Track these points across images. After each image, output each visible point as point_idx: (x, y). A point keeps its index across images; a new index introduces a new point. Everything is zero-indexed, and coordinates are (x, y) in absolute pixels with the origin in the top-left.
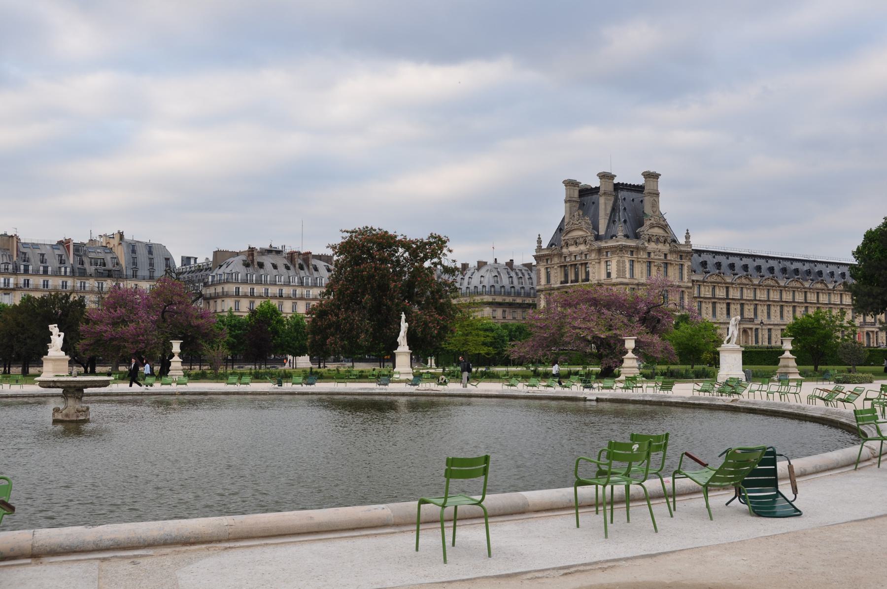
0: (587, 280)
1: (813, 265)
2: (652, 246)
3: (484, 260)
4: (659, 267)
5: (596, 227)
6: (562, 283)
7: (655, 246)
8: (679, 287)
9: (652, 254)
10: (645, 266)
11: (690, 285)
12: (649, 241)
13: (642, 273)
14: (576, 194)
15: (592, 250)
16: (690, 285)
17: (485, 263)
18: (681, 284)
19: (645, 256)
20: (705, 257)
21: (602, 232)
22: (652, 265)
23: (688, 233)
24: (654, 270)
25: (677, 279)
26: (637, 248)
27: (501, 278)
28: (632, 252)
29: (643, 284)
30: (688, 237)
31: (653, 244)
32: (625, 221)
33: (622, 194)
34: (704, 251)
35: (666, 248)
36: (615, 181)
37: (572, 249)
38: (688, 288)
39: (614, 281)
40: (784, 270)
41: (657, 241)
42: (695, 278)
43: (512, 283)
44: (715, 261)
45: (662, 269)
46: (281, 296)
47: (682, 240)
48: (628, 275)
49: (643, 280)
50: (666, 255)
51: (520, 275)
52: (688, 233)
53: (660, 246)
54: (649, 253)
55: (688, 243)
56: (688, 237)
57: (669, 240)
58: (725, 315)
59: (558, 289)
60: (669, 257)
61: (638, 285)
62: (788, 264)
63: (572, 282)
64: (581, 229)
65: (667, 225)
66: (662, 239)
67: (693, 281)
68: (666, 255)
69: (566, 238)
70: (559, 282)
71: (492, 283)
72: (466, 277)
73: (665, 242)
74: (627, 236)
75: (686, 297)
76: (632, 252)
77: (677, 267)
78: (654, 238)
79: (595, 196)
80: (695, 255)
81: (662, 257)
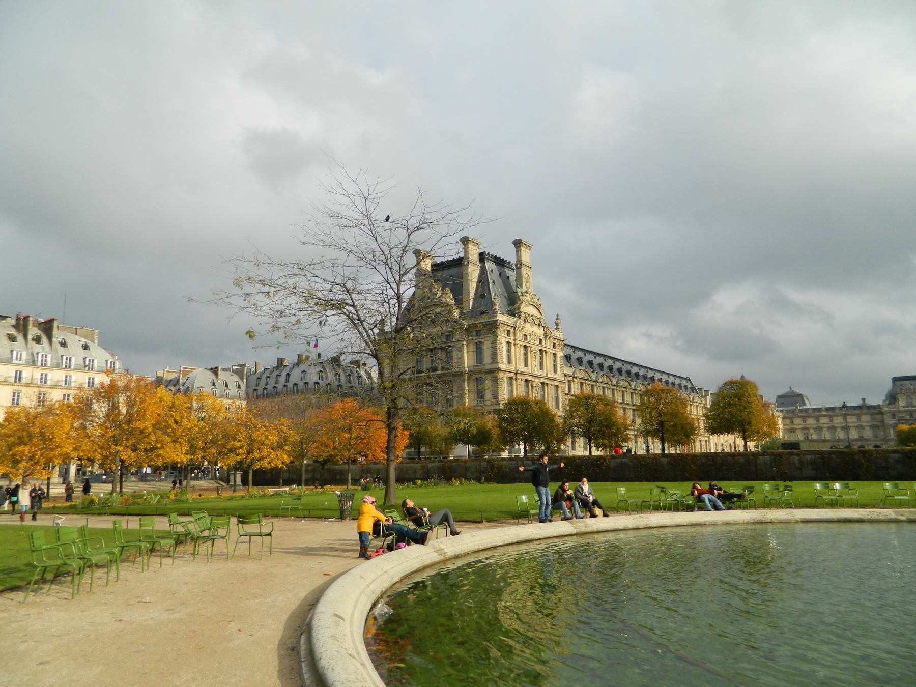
2: (528, 328)
9: (528, 338)
14: (429, 268)
19: (522, 338)
27: (326, 374)
29: (522, 373)
35: (540, 332)
39: (487, 367)
40: (629, 373)
43: (339, 380)
50: (540, 340)
51: (348, 372)
53: (535, 328)
62: (629, 367)
67: (565, 375)
71: (316, 379)
74: (503, 313)
75: (560, 393)
78: (530, 319)
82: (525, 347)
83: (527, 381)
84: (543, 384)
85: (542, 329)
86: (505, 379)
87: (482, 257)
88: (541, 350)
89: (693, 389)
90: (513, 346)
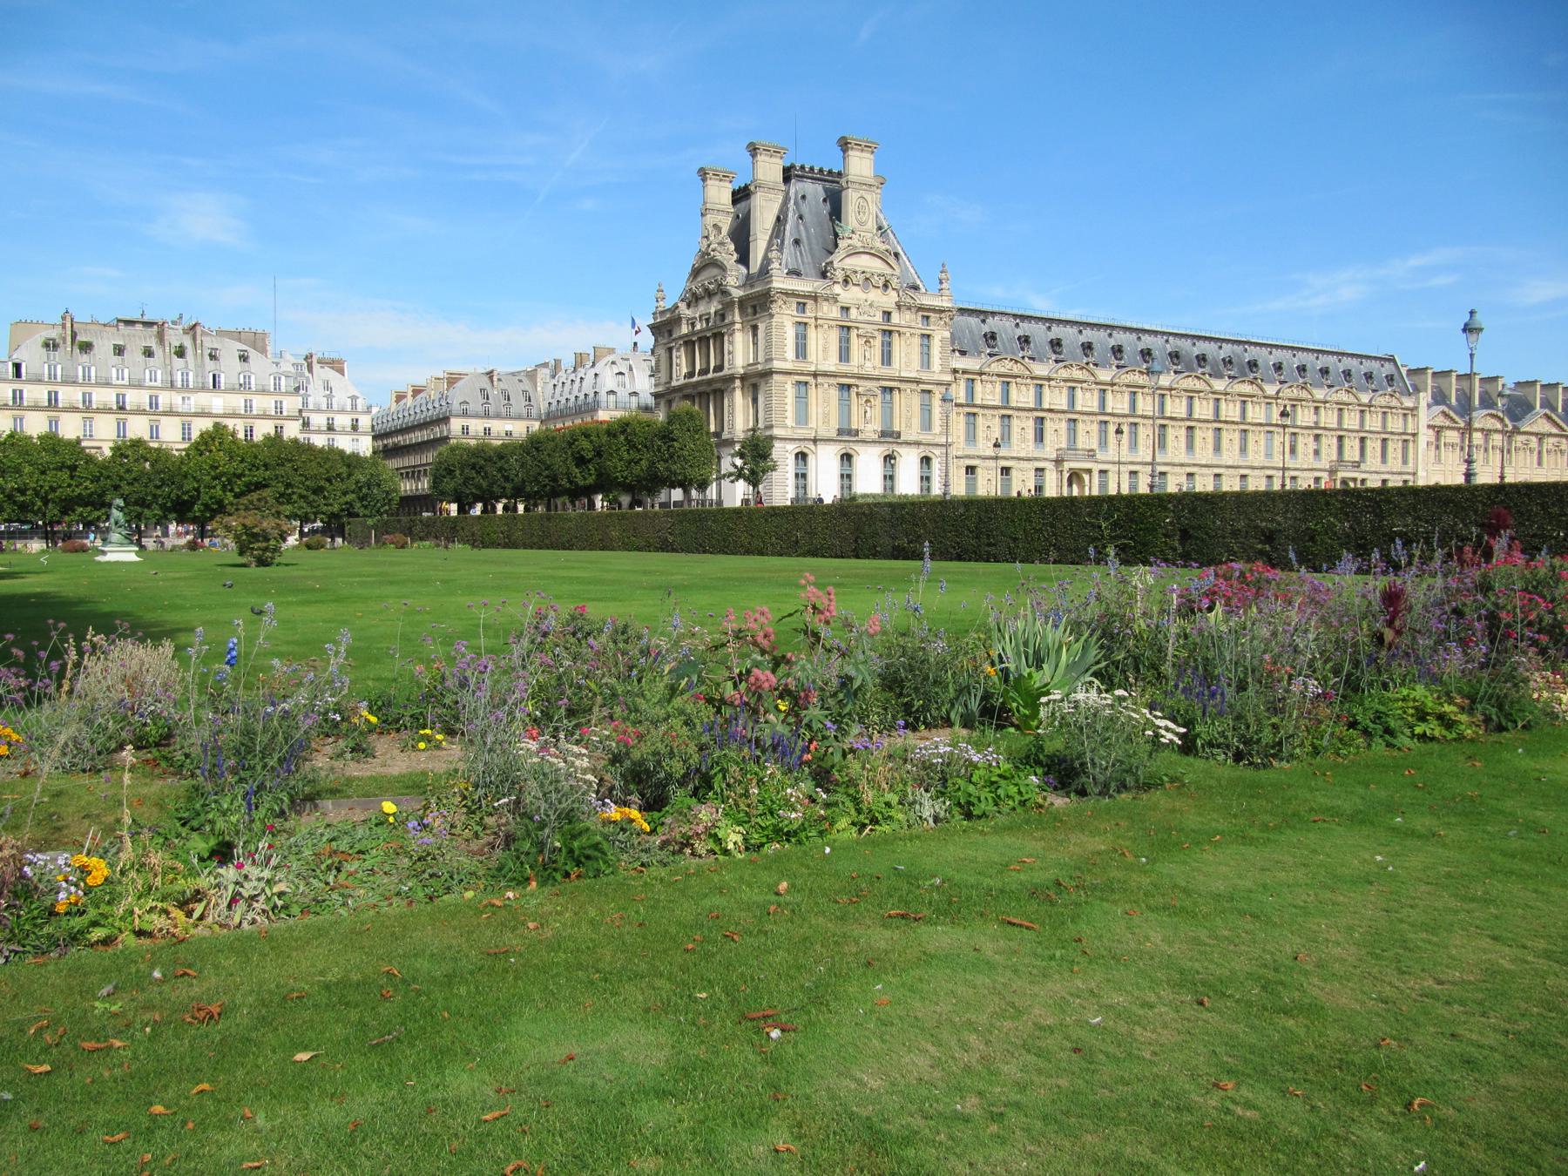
0: (719, 368)
9: (854, 313)
10: (834, 336)
11: (948, 378)
13: (825, 350)
16: (948, 378)
18: (924, 376)
19: (835, 312)
20: (993, 324)
22: (854, 333)
24: (856, 344)
25: (916, 364)
26: (815, 298)
29: (826, 375)
32: (797, 242)
33: (796, 187)
34: (993, 314)
38: (939, 384)
42: (960, 363)
45: (877, 343)
46: (122, 408)
48: (790, 353)
49: (831, 363)
50: (887, 314)
53: (875, 295)
54: (846, 309)
57: (894, 282)
58: (1031, 443)
60: (895, 318)
61: (815, 375)
67: (955, 371)
68: (887, 314)
73: (886, 286)
74: (795, 273)
77: (917, 341)
80: (974, 321)
81: (879, 317)
85: (894, 294)
86: (789, 387)
87: (788, 175)
90: (811, 333)
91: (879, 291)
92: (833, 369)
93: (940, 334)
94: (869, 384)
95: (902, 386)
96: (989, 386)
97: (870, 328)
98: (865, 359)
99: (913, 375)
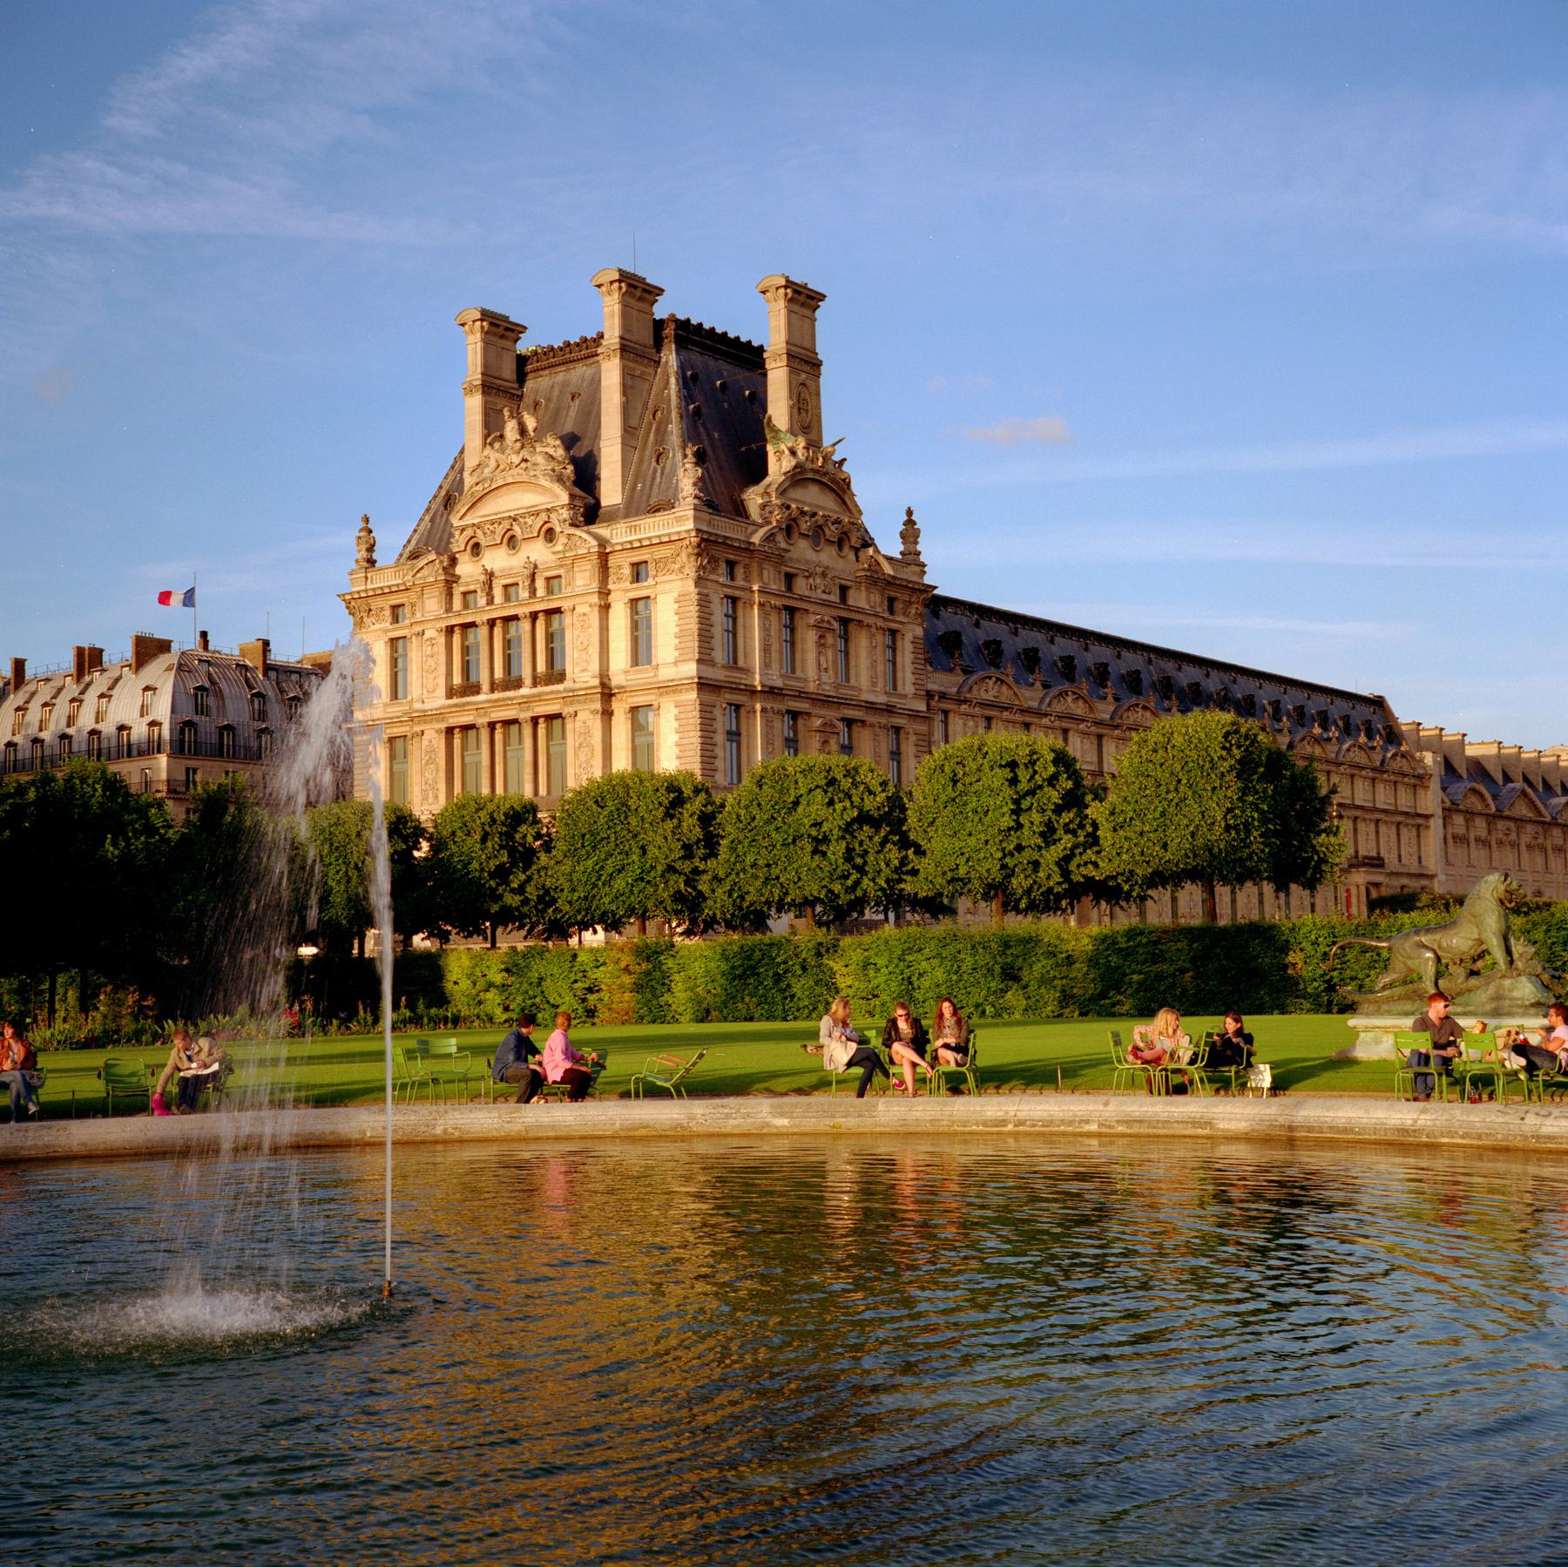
0: (555, 675)
1: (1226, 677)
3: (159, 635)
4: (822, 630)
5: (584, 476)
6: (451, 693)
7: (810, 555)
8: (889, 710)
9: (801, 586)
11: (921, 706)
12: (788, 531)
14: (508, 370)
15: (576, 558)
16: (921, 706)
17: (164, 646)
19: (777, 585)
21: (611, 492)
22: (801, 622)
23: (910, 522)
24: (808, 639)
28: (731, 565)
30: (910, 532)
31: (803, 544)
36: (661, 310)
37: (497, 559)
38: (914, 715)
41: (817, 536)
44: (981, 636)
47: (889, 544)
50: (844, 590)
52: (910, 522)
53: (828, 556)
54: (790, 578)
55: (911, 557)
56: (910, 532)
59: (439, 715)
60: (859, 599)
63: (493, 688)
64: (531, 485)
65: (847, 483)
66: (831, 532)
67: (929, 695)
68: (844, 590)
69: (468, 520)
70: (442, 691)
72: (91, 697)
76: (731, 565)
78: (805, 525)
79: (580, 371)
81: (835, 598)
82: (791, 611)
83: (795, 715)
84: (849, 722)
85: (852, 556)
88: (845, 622)
89: (1393, 735)
91: (833, 550)
92: (779, 683)
93: (912, 632)
94: (832, 714)
95: (871, 719)
96: (971, 723)
97: (827, 615)
98: (814, 668)
99: (882, 699)
